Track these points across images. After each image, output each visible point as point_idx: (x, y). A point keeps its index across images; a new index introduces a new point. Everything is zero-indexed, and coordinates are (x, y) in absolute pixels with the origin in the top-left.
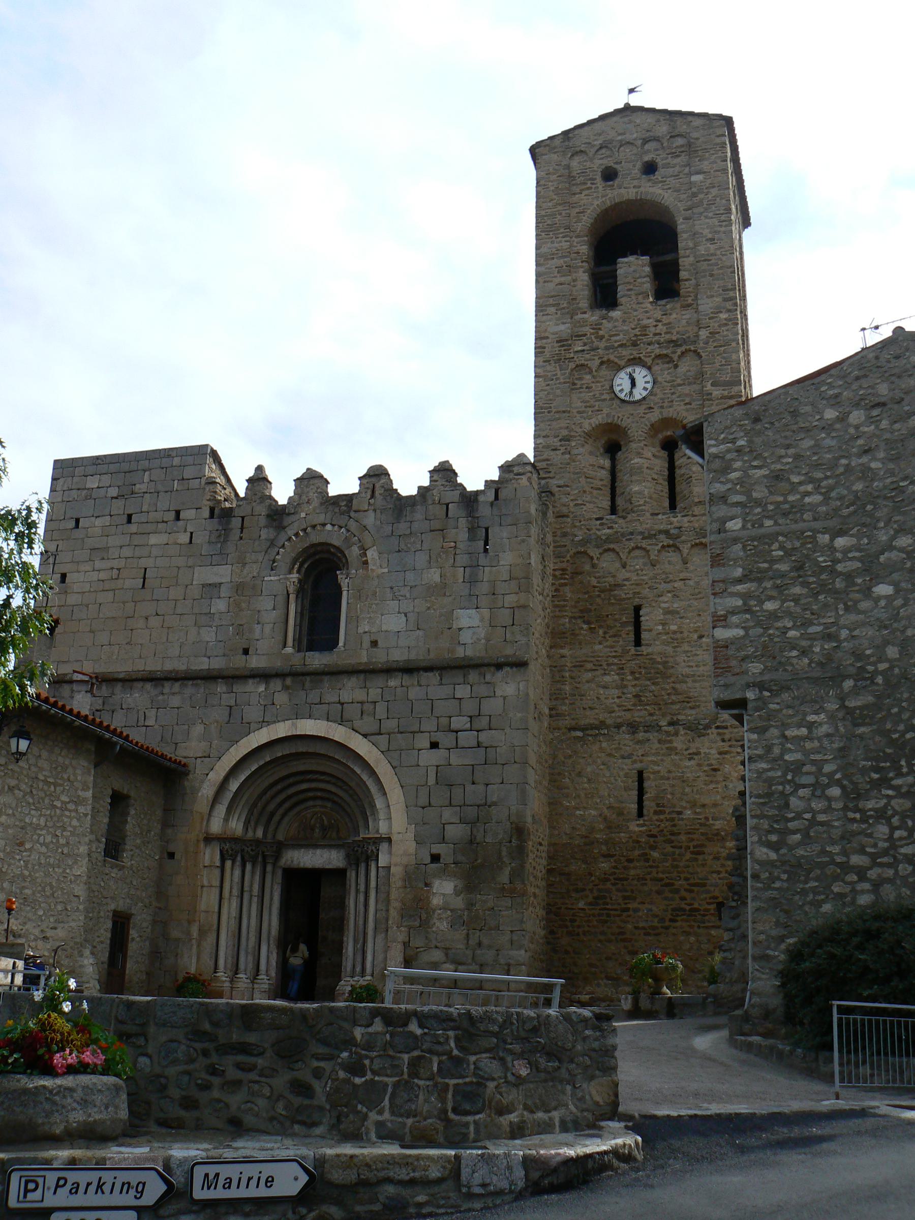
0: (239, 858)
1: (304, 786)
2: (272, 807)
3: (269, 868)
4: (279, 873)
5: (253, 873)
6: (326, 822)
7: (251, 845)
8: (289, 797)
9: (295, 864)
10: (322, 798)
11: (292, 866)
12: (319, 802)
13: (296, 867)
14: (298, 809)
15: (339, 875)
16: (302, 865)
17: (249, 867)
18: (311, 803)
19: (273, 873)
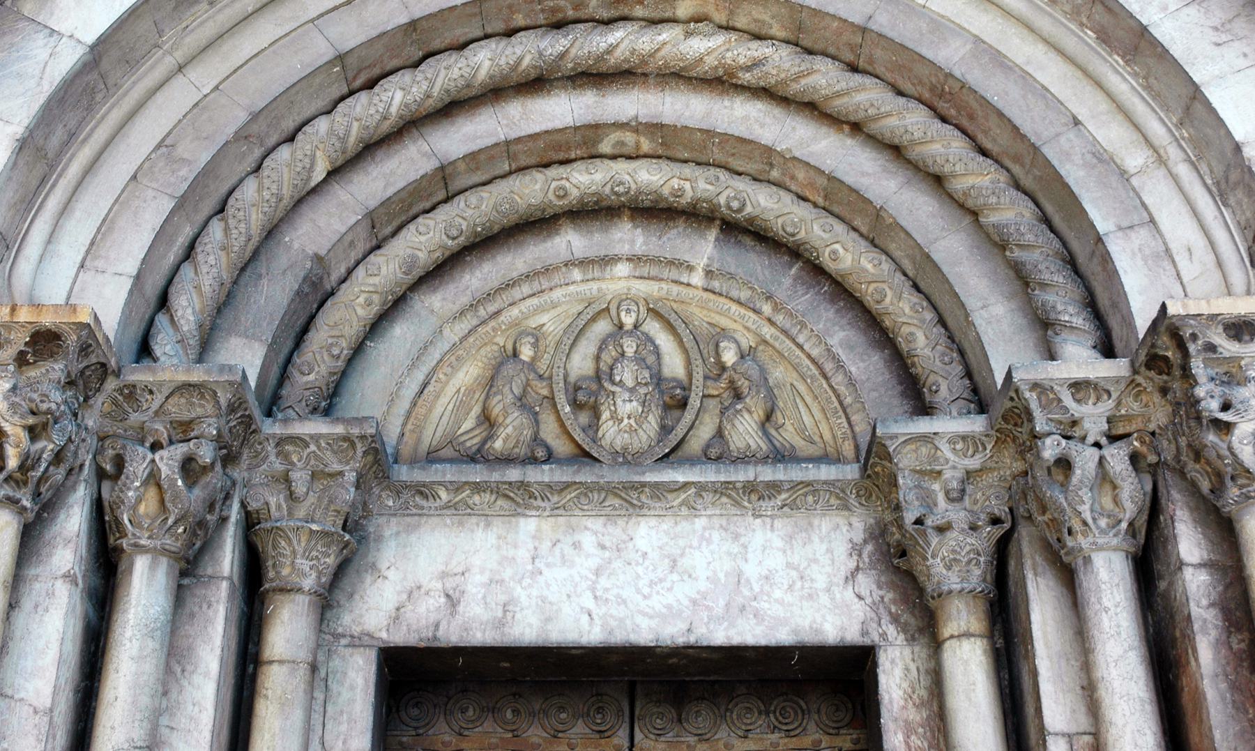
0: (73, 521)
1: (560, 110)
2: (327, 225)
3: (287, 631)
4: (357, 682)
5: (174, 654)
6: (674, 365)
7: (184, 430)
8: (442, 186)
9: (475, 625)
10: (655, 211)
11: (453, 634)
12: (627, 237)
13: (481, 636)
14: (478, 277)
15: (835, 679)
16: (527, 629)
17: (145, 590)
18: (570, 241)
19: (316, 673)
